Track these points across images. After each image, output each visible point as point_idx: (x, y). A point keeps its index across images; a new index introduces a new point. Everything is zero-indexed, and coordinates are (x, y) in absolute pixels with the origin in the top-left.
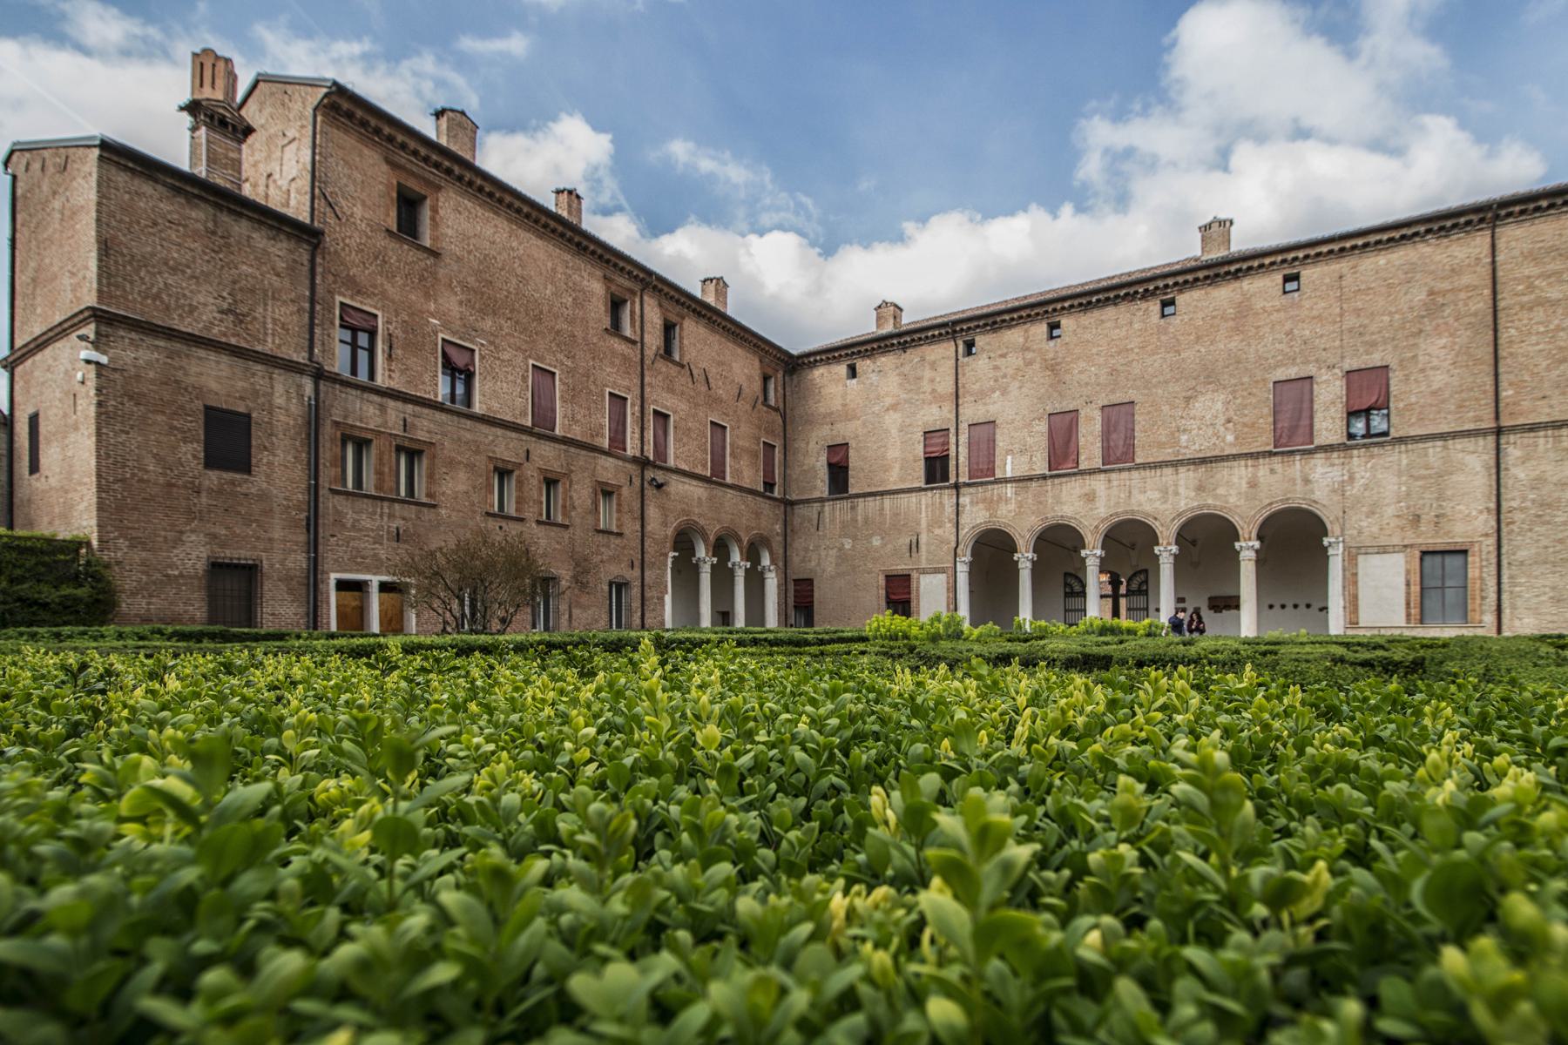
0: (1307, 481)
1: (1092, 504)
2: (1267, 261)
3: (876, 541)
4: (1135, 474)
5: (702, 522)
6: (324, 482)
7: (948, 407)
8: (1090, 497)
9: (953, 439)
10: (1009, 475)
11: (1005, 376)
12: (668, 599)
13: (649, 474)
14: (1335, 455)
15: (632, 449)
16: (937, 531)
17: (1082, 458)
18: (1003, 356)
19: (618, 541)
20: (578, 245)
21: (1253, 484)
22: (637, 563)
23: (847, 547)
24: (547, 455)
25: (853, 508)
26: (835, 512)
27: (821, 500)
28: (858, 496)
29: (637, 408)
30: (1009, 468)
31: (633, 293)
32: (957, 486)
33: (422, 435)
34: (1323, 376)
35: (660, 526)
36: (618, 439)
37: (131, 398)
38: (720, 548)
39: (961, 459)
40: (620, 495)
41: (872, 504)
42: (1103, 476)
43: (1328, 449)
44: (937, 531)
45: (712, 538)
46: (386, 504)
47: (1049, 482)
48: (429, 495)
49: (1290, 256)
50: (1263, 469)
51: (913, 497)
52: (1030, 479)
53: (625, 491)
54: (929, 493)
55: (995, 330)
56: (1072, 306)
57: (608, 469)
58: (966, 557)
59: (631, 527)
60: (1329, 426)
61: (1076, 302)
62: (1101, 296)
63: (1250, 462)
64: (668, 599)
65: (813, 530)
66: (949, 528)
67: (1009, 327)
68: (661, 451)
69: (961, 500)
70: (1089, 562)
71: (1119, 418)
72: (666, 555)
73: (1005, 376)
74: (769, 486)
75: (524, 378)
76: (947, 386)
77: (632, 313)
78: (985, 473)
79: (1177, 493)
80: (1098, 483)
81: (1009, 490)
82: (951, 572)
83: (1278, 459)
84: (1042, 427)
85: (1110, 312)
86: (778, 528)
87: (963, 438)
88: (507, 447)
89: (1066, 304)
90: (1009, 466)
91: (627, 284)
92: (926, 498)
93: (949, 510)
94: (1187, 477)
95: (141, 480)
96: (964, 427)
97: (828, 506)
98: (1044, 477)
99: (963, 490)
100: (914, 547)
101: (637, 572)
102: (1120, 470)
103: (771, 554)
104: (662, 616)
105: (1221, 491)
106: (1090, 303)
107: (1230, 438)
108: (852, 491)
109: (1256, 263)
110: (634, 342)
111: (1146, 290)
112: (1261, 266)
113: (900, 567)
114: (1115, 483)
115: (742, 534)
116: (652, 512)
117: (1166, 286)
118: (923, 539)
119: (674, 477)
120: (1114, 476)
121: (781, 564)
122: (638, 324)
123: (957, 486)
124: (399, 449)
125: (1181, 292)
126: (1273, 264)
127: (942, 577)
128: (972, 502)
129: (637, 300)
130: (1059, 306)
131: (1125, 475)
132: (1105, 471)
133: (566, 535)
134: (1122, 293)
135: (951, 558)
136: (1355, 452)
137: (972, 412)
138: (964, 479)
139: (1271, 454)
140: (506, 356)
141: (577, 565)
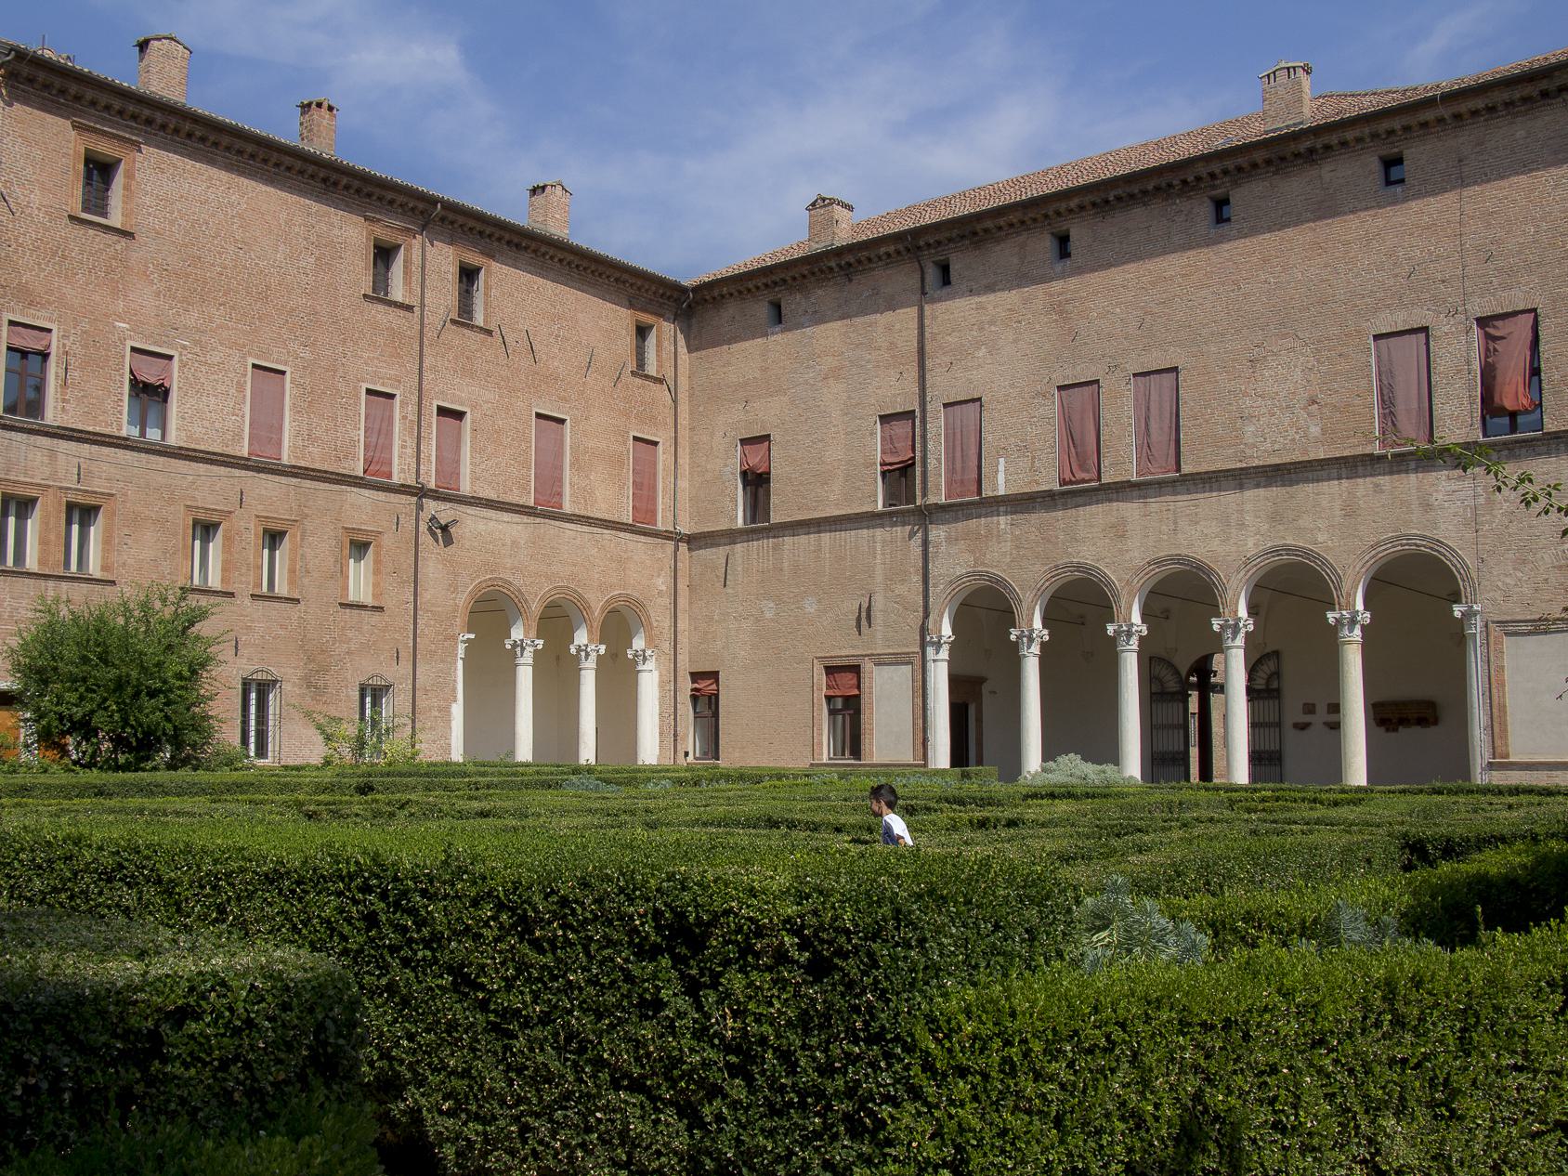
1: (1124, 548)
8: (1119, 531)
10: (1002, 492)
11: (992, 323)
12: (457, 710)
16: (900, 589)
19: (376, 617)
20: (325, 180)
22: (406, 655)
23: (769, 615)
29: (411, 409)
30: (1001, 478)
34: (1443, 328)
35: (447, 586)
39: (932, 462)
40: (379, 546)
44: (900, 589)
45: (536, 607)
46: (51, 583)
49: (1385, 125)
53: (388, 540)
56: (1082, 208)
57: (362, 507)
59: (397, 597)
60: (1458, 419)
66: (917, 579)
67: (998, 241)
72: (454, 638)
77: (407, 263)
79: (1242, 525)
82: (918, 661)
84: (1052, 408)
94: (1256, 499)
96: (935, 408)
100: (865, 617)
101: (405, 667)
104: (446, 736)
105: (1305, 522)
106: (1107, 202)
107: (1315, 430)
110: (409, 308)
111: (1184, 182)
112: (1344, 144)
113: (845, 650)
117: (1213, 176)
118: (879, 603)
119: (470, 510)
122: (416, 278)
125: (1236, 184)
126: (1359, 140)
128: (948, 539)
137: (944, 385)
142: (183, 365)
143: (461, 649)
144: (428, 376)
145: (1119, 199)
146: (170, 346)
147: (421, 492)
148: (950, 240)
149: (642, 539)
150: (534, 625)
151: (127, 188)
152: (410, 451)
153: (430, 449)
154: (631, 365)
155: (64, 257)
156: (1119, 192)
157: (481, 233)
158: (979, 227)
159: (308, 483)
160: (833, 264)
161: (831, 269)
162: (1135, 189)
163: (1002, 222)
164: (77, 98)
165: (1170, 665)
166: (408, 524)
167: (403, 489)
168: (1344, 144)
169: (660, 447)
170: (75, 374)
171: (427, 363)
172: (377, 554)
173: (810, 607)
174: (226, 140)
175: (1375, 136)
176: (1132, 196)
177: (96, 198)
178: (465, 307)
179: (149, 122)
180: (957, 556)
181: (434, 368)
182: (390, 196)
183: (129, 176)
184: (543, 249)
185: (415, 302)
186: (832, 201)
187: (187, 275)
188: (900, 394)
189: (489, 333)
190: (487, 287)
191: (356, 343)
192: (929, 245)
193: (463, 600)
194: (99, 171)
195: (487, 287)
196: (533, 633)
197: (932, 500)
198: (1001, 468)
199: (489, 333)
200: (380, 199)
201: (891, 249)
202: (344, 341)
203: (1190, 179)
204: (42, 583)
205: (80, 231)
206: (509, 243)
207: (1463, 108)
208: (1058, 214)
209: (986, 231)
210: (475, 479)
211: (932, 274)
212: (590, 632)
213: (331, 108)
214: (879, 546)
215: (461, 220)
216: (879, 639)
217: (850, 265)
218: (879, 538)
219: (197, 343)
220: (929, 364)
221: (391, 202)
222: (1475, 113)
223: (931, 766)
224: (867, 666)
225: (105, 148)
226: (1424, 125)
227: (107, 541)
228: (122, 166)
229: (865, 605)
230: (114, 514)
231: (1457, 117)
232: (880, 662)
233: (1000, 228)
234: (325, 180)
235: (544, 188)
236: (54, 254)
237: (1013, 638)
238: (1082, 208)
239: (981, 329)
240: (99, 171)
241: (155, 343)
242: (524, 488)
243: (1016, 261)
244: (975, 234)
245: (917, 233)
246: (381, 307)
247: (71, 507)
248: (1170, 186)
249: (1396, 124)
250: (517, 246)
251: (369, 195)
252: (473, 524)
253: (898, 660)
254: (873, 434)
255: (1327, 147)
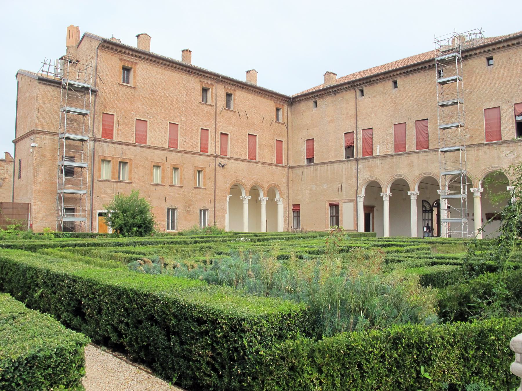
0: (499, 158)
1: (412, 169)
2: (477, 52)
3: (325, 186)
4: (429, 154)
5: (243, 180)
6: (96, 178)
7: (353, 121)
8: (411, 165)
9: (355, 137)
10: (378, 154)
11: (375, 106)
12: (227, 216)
13: (219, 160)
14: (511, 145)
15: (211, 151)
16: (350, 182)
17: (407, 146)
18: (374, 97)
19: (204, 191)
20: (189, 71)
21: (477, 160)
22: (212, 201)
23: (314, 189)
24: (174, 158)
25: (316, 170)
26: (309, 171)
27: (303, 166)
28: (318, 164)
29: (213, 133)
30: (378, 150)
31: (212, 85)
32: (357, 160)
33: (128, 157)
34: (504, 107)
35: (224, 183)
36: (204, 149)
37: (43, 156)
38: (254, 191)
39: (359, 146)
40: (205, 172)
41: (324, 168)
42: (416, 155)
43: (507, 142)
44: (350, 182)
45: (249, 188)
47: (395, 157)
48: (130, 179)
49: (486, 49)
50: (482, 151)
51: (340, 165)
52: (386, 156)
53: (207, 170)
54: (346, 163)
55: (371, 85)
56: (400, 74)
57: (200, 161)
58: (362, 193)
59: (210, 185)
61: (402, 72)
62: (411, 69)
63: (476, 148)
64: (227, 216)
65: (300, 180)
67: (377, 83)
68: (224, 151)
69: (359, 166)
70: (412, 198)
71: (423, 123)
72: (226, 196)
73: (375, 106)
74: (279, 160)
75: (166, 128)
76: (352, 112)
77: (212, 93)
78: (368, 151)
80: (414, 158)
81: (378, 161)
82: (355, 202)
83: (487, 147)
84: (391, 131)
85: (416, 76)
86: (284, 180)
87: (360, 136)
88: (158, 156)
89: (398, 73)
90: (378, 151)
91: (209, 82)
92: (344, 166)
93: (355, 171)
95: (45, 182)
96: (360, 131)
97: (306, 170)
98: (392, 155)
99: (359, 162)
100: (340, 189)
101: (212, 204)
102: (423, 152)
103: (280, 192)
104: (224, 223)
106: (407, 72)
108: (315, 162)
109: (473, 53)
110: (212, 106)
111: (430, 66)
112: (476, 54)
113: (334, 199)
114: (421, 158)
115: (264, 184)
116: (219, 177)
118: (344, 185)
119: (231, 161)
120: (420, 154)
121: (286, 198)
122: (214, 97)
123: (357, 160)
124: (120, 162)
126: (480, 53)
127: (352, 204)
128: (363, 167)
129: (214, 88)
130: (395, 74)
131: (425, 154)
132: (417, 153)
133: (182, 190)
134: (420, 67)
135: (355, 195)
136: (519, 144)
137: (363, 124)
138: (361, 156)
139: (484, 145)
140: (159, 121)
141: (186, 203)
142: (150, 123)
143: (228, 200)
144: (218, 125)
145: (411, 71)
146: (147, 118)
147: (216, 156)
148: (364, 83)
149: (278, 168)
150: (248, 192)
151: (134, 75)
152: (213, 145)
153: (219, 144)
154: (275, 120)
155: (117, 95)
156: (411, 69)
157: (232, 84)
158: (371, 80)
159: (185, 155)
160: (331, 91)
161: (330, 92)
162: (416, 68)
163: (378, 78)
164: (120, 52)
165: (428, 202)
166: (213, 165)
167: (211, 156)
168: (476, 54)
169: (283, 143)
170: (121, 127)
171: (218, 121)
172: (204, 173)
173: (325, 186)
174: (161, 61)
175: (484, 52)
176: (415, 70)
177: (126, 80)
178: (228, 105)
179: (140, 57)
180: (367, 172)
181: (220, 122)
182: (206, 75)
183: (135, 72)
184: (250, 88)
185: (214, 104)
186: (331, 73)
187: (151, 99)
188: (349, 127)
189: (235, 112)
190: (234, 99)
191: (198, 116)
192: (357, 85)
193: (228, 186)
194: (127, 70)
195: (234, 99)
196: (248, 194)
197: (359, 157)
198: (378, 148)
199: (235, 112)
200: (204, 76)
201: (347, 86)
202: (194, 116)
203: (431, 65)
204: (113, 183)
205: (121, 88)
206: (240, 87)
207: (510, 43)
208: (394, 75)
209: (374, 80)
210: (231, 152)
211: (359, 93)
212: (264, 194)
213: (190, 51)
214: (344, 170)
215: (226, 81)
216: (344, 195)
217: (335, 91)
218: (344, 167)
219: (154, 117)
220: (358, 118)
221: (207, 77)
222: (513, 44)
223: (359, 231)
224: (341, 204)
225: (128, 65)
226: (499, 48)
227: (130, 172)
228: (133, 70)
229: (340, 186)
230: (132, 164)
231: (508, 46)
232: (344, 201)
233: (377, 80)
234: (189, 71)
235: (250, 71)
236: (115, 94)
237: (381, 195)
238: (400, 74)
239: (372, 108)
240: (127, 70)
241: (143, 118)
242: (245, 154)
243: (382, 89)
244: (370, 81)
245: (354, 82)
246: (204, 106)
247: (120, 162)
248: (426, 67)
249: (491, 48)
250: (243, 88)
251: (201, 75)
252: (231, 165)
253: (350, 201)
254: (342, 138)
255: (471, 55)
